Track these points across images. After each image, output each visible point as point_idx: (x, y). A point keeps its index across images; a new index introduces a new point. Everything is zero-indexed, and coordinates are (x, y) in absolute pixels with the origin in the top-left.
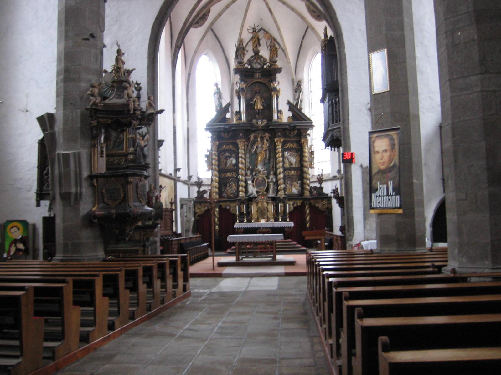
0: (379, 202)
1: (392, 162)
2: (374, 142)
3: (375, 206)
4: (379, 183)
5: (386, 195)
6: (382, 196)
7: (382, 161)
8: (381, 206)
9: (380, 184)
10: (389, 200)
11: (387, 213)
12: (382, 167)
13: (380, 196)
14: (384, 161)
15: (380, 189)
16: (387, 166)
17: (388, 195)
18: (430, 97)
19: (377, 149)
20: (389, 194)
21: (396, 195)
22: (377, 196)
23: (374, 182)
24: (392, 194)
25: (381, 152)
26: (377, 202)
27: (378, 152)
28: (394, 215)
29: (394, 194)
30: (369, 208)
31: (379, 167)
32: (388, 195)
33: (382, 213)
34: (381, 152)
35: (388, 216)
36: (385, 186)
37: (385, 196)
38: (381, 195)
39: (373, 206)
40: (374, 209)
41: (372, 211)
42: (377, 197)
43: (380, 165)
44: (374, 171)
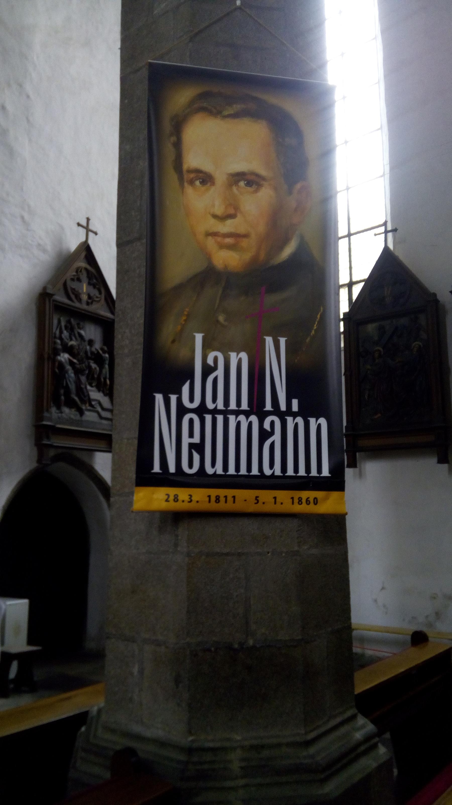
0: (199, 448)
1: (286, 241)
2: (178, 126)
3: (172, 469)
4: (199, 338)
5: (245, 406)
6: (215, 412)
7: (227, 227)
8: (209, 470)
9: (207, 346)
10: (264, 435)
11: (252, 508)
12: (227, 259)
13: (201, 410)
14: (242, 230)
15: (207, 370)
16: (255, 259)
17: (256, 408)
18: (22, 218)
19: (193, 160)
20: (268, 407)
21: (306, 412)
22: (182, 411)
23: (168, 329)
24: (283, 407)
25: (220, 178)
26: (186, 441)
27: (206, 179)
28: (295, 523)
29: (295, 406)
30: (133, 476)
31: (209, 258)
32: (256, 408)
33: (213, 507)
34: (220, 178)
35: (251, 526)
36: (240, 359)
37: (237, 413)
38: (210, 405)
39: (157, 468)
40: (165, 480)
41: (155, 499)
42: (187, 417)
43: (211, 243)
44: (177, 268)
